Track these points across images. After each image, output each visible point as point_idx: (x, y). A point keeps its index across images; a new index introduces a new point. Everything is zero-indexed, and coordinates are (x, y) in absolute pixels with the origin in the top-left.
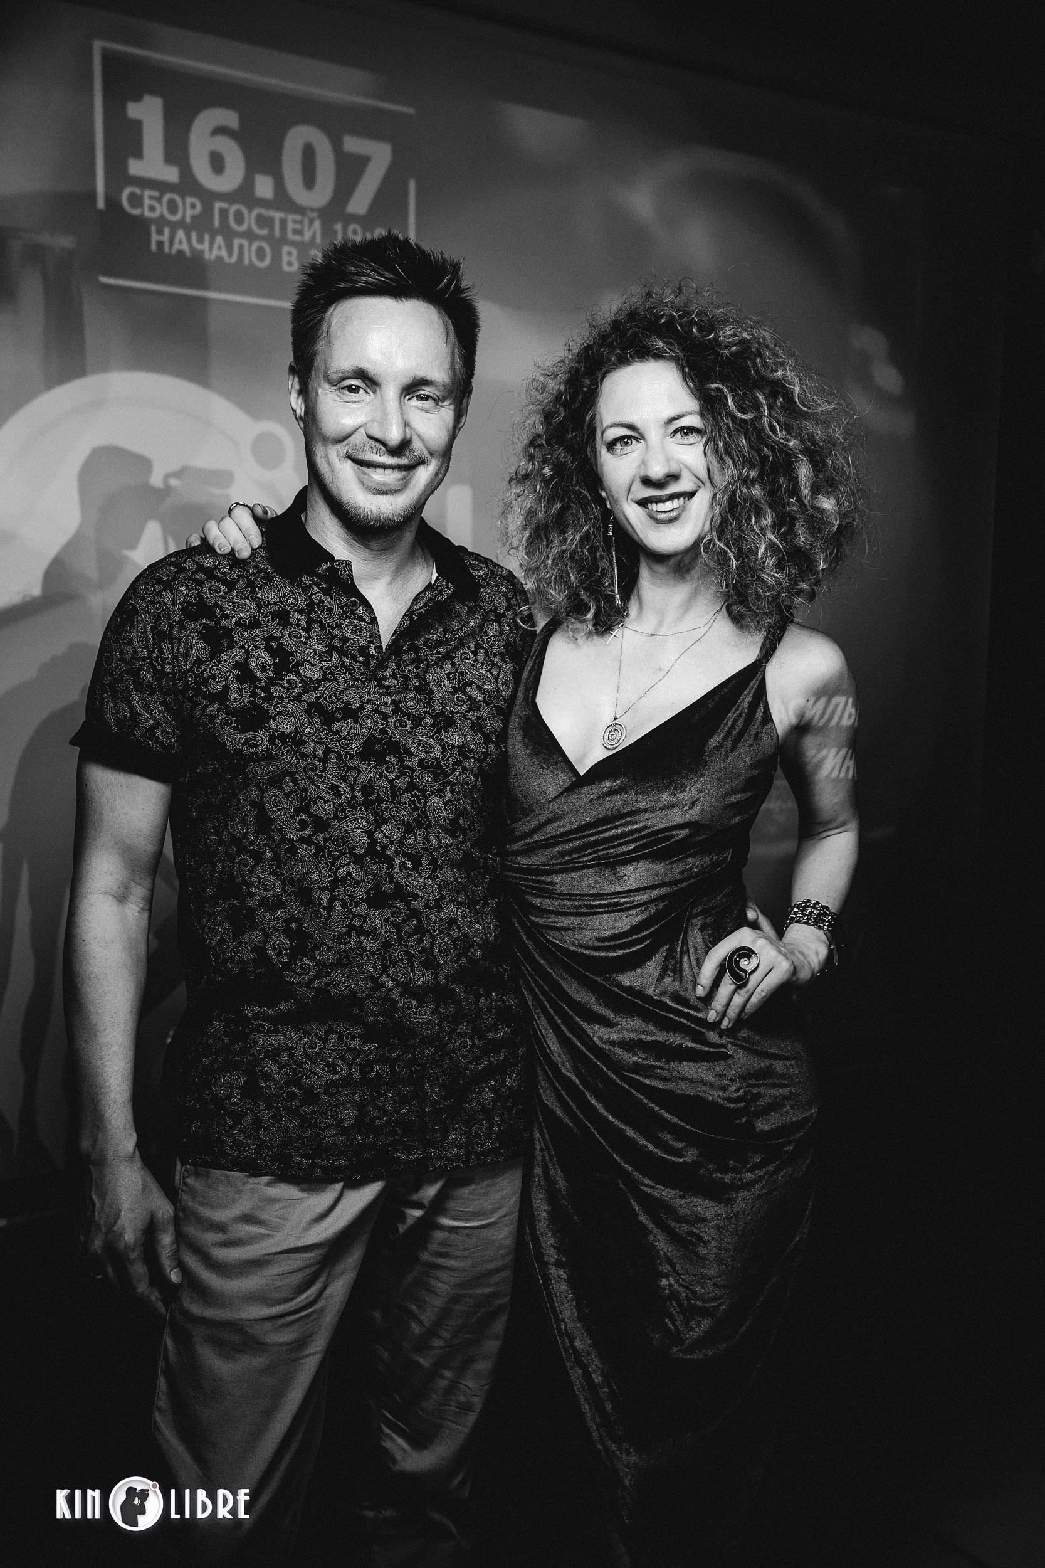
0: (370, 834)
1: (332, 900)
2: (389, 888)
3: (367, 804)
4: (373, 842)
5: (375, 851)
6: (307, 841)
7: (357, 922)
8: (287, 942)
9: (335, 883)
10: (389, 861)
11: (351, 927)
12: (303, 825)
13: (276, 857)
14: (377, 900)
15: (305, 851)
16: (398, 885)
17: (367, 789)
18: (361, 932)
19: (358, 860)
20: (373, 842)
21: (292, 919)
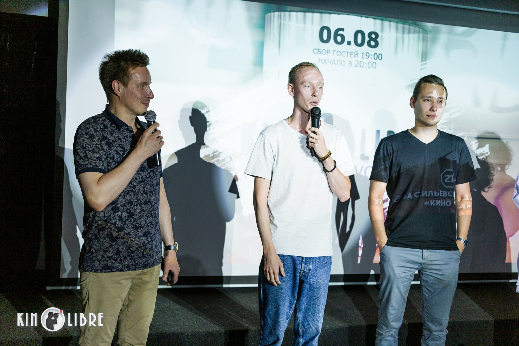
0: (144, 188)
3: (143, 181)
4: (144, 190)
5: (145, 192)
10: (147, 194)
16: (149, 200)
17: (142, 178)
20: (144, 190)
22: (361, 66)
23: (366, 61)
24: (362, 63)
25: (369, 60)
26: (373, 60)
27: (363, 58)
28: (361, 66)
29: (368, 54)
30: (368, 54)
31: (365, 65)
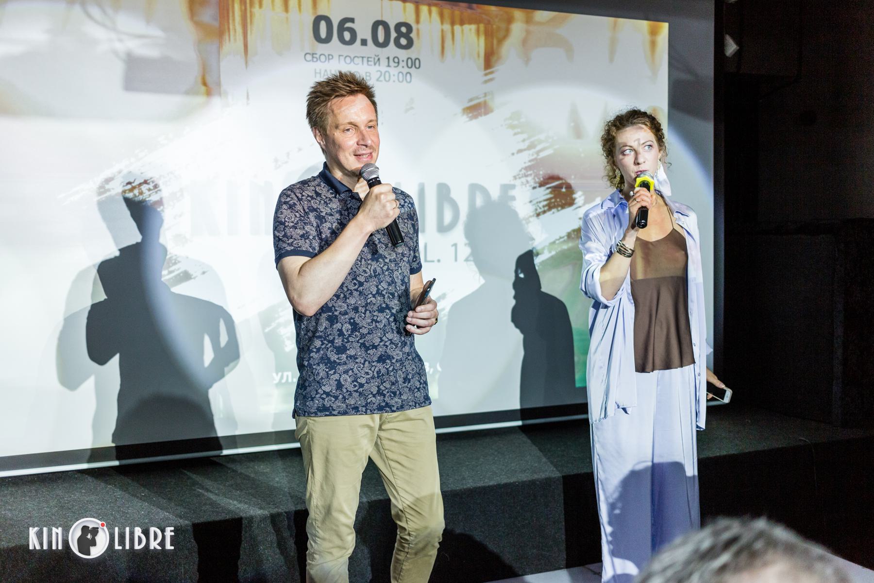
0: (377, 286)
1: (366, 310)
2: (384, 305)
3: (375, 276)
4: (378, 289)
5: (379, 293)
6: (356, 290)
7: (375, 318)
8: (350, 327)
9: (367, 304)
10: (384, 296)
11: (373, 320)
12: (355, 284)
13: (345, 296)
14: (381, 310)
15: (356, 294)
16: (387, 305)
18: (377, 321)
19: (374, 296)
20: (378, 289)
21: (352, 318)
22: (387, 79)
23: (393, 71)
24: (387, 74)
25: (400, 68)
26: (406, 70)
27: (389, 66)
28: (387, 79)
29: (396, 60)
30: (396, 60)
31: (392, 78)
